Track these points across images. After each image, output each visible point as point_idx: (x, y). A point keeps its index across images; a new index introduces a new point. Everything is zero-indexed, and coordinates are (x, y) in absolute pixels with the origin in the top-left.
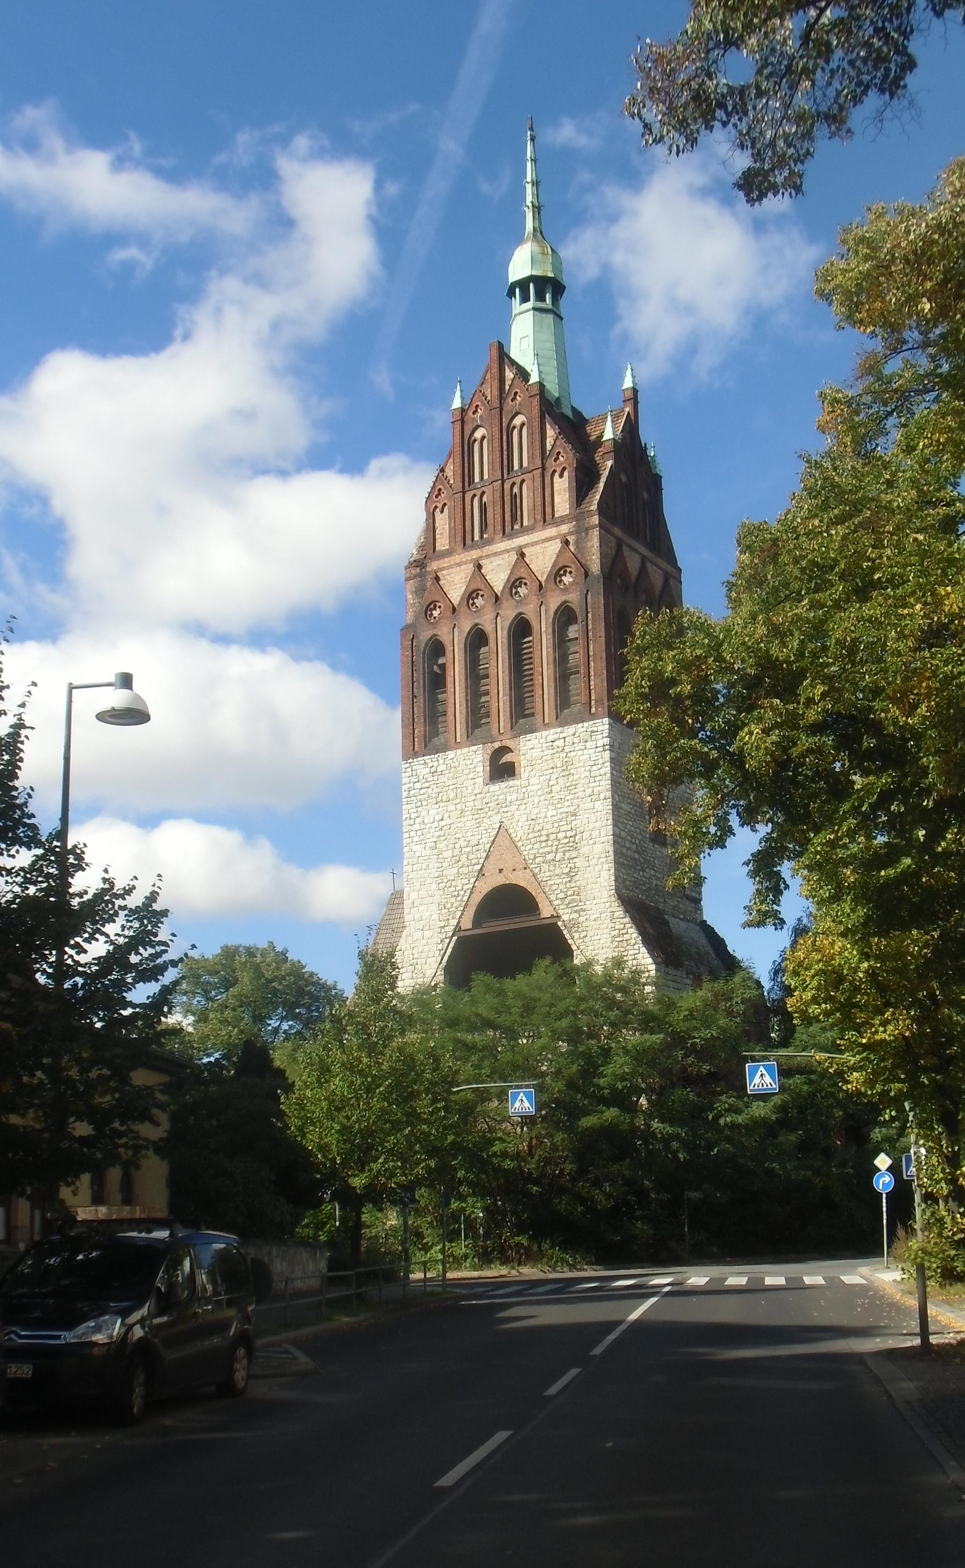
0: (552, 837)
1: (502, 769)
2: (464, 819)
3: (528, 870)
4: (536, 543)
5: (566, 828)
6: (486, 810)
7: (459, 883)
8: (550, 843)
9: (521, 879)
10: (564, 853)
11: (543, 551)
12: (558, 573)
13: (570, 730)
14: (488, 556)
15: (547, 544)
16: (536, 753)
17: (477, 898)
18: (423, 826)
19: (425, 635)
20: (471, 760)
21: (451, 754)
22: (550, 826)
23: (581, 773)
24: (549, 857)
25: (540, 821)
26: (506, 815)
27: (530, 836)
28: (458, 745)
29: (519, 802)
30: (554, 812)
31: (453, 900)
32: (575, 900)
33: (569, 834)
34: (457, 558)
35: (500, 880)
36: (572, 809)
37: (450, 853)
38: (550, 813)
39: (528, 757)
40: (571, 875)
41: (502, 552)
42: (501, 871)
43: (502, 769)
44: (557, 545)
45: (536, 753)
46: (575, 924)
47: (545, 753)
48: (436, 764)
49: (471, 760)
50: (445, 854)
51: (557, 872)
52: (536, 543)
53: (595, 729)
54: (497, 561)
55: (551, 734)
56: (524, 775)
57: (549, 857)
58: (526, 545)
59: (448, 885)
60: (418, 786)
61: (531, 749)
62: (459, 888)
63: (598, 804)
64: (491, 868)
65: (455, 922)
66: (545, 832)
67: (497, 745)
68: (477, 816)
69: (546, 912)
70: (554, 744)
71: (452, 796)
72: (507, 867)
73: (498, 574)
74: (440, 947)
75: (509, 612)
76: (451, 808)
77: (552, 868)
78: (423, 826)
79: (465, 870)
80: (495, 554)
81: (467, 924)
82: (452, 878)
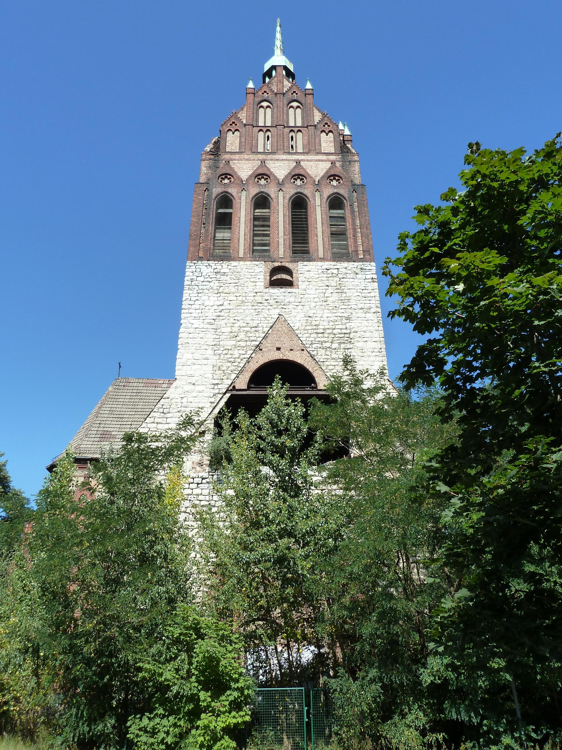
2: (243, 308)
3: (305, 352)
4: (311, 161)
5: (341, 327)
6: (266, 304)
7: (236, 353)
8: (326, 335)
13: (345, 264)
14: (271, 160)
15: (319, 163)
17: (254, 366)
18: (202, 307)
19: (216, 190)
21: (234, 263)
25: (316, 319)
26: (284, 310)
27: (307, 328)
29: (297, 304)
31: (229, 364)
33: (345, 331)
34: (246, 157)
36: (346, 315)
37: (229, 329)
41: (283, 160)
42: (278, 349)
44: (328, 165)
47: (321, 275)
48: (220, 267)
50: (223, 330)
51: (334, 356)
52: (311, 161)
53: (365, 268)
54: (278, 164)
55: (326, 264)
57: (328, 345)
58: (302, 160)
59: (225, 352)
62: (237, 356)
63: (368, 315)
64: (267, 345)
65: (230, 382)
67: (276, 264)
68: (257, 307)
70: (329, 271)
73: (280, 168)
74: (212, 400)
75: (290, 190)
76: (232, 298)
77: (328, 353)
78: (202, 307)
79: (243, 344)
80: (277, 160)
81: (242, 383)
82: (229, 348)
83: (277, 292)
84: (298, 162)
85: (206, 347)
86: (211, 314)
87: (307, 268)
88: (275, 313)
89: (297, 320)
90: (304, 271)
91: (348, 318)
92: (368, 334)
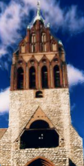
1: (38, 95)
9: (44, 119)
11: (50, 56)
12: (55, 60)
17: (31, 122)
20: (32, 92)
21: (25, 91)
23: (62, 99)
28: (26, 89)
32: (61, 125)
35: (38, 119)
40: (59, 119)
46: (58, 130)
55: (53, 90)
56: (46, 97)
61: (47, 92)
64: (35, 116)
69: (51, 126)
73: (38, 57)
75: (42, 65)
81: (28, 127)
83: (38, 99)
84: (44, 55)
86: (18, 107)
88: (37, 106)
89: (44, 107)
90: (46, 92)
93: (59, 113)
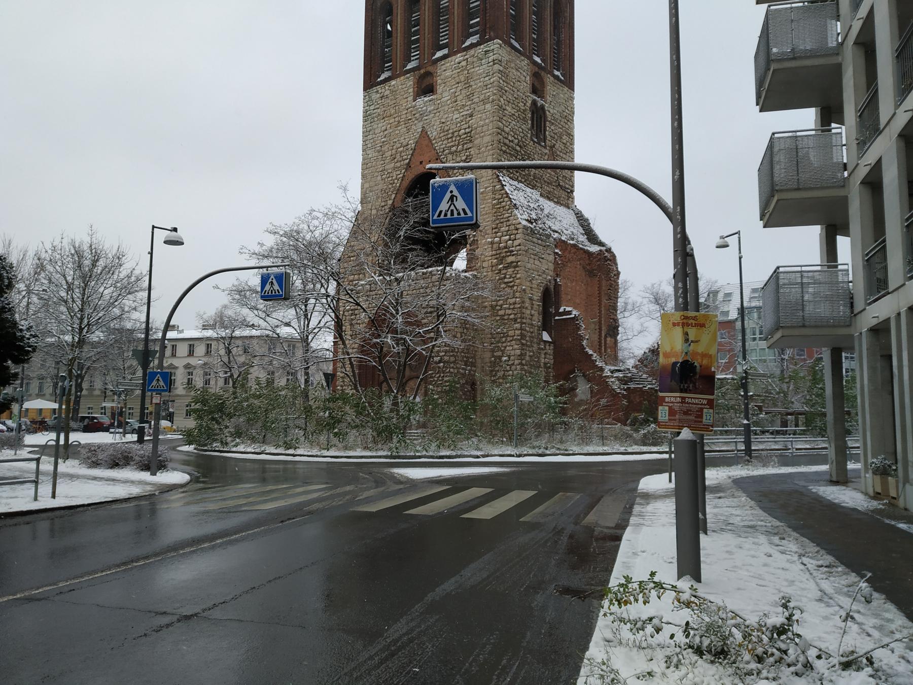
0: (456, 134)
10: (463, 145)
16: (448, 73)
17: (406, 183)
22: (454, 126)
23: (476, 85)
24: (454, 148)
30: (458, 116)
33: (467, 130)
38: (455, 117)
39: (442, 77)
43: (426, 87)
45: (448, 73)
49: (405, 85)
56: (439, 91)
57: (454, 148)
60: (372, 107)
65: (390, 202)
66: (451, 131)
71: (393, 111)
72: (425, 158)
79: (398, 164)
85: (376, 174)
87: (443, 68)
91: (471, 116)
92: (485, 128)
93: (470, 138)
